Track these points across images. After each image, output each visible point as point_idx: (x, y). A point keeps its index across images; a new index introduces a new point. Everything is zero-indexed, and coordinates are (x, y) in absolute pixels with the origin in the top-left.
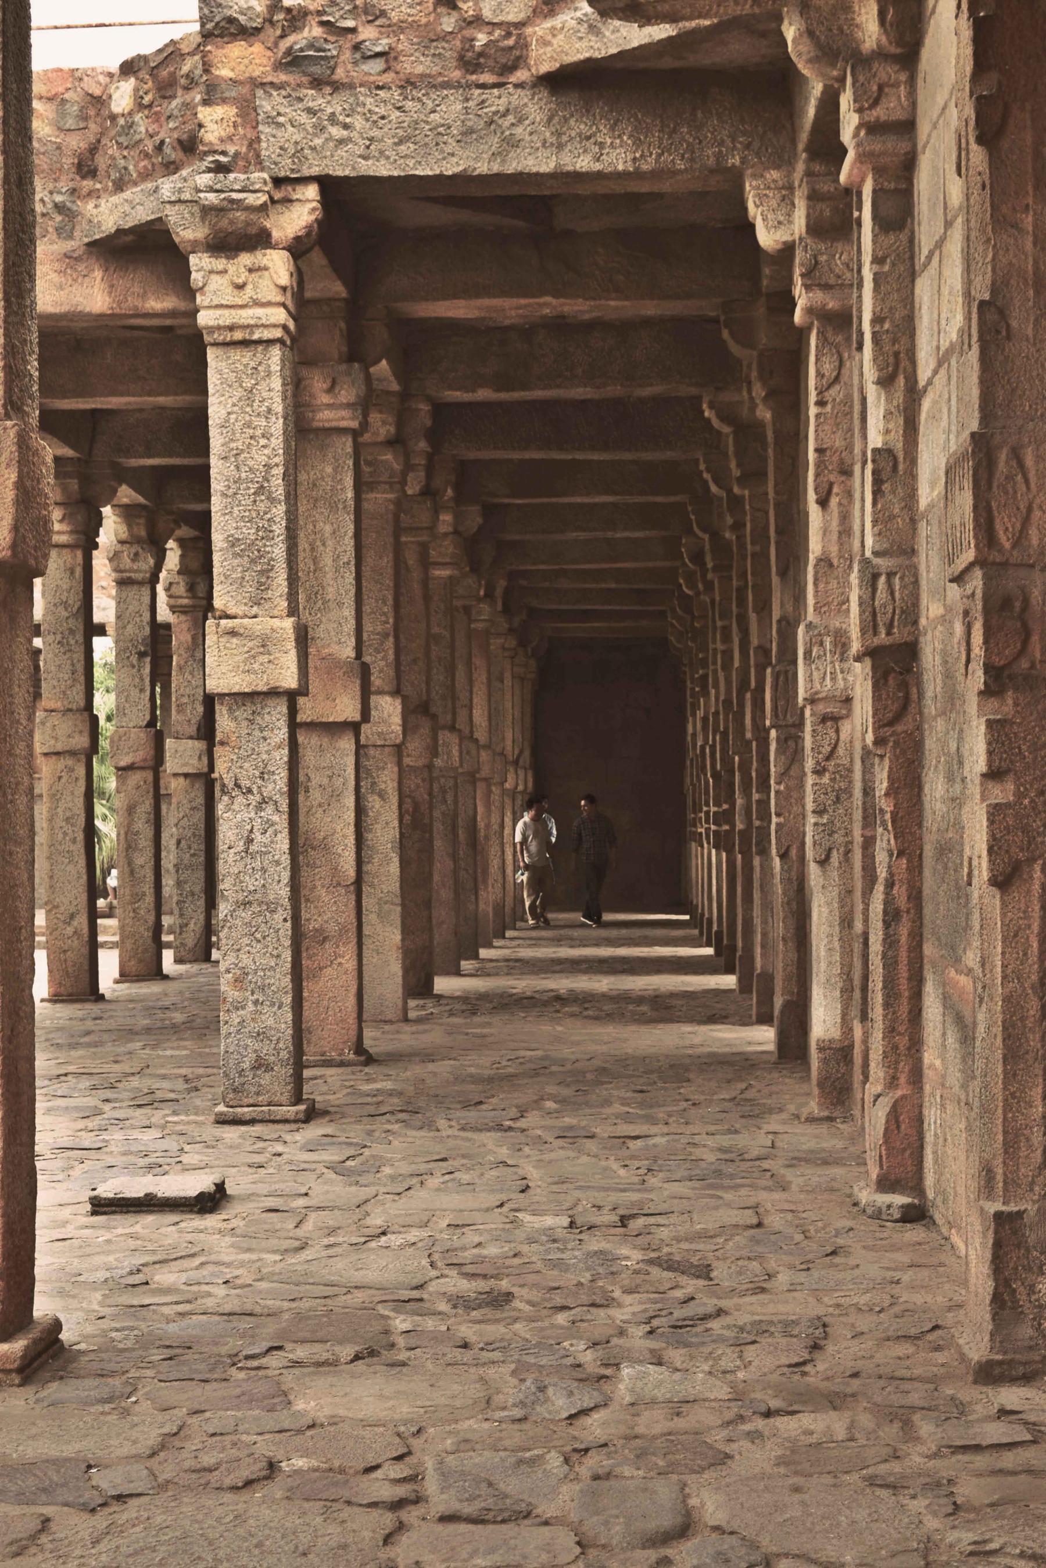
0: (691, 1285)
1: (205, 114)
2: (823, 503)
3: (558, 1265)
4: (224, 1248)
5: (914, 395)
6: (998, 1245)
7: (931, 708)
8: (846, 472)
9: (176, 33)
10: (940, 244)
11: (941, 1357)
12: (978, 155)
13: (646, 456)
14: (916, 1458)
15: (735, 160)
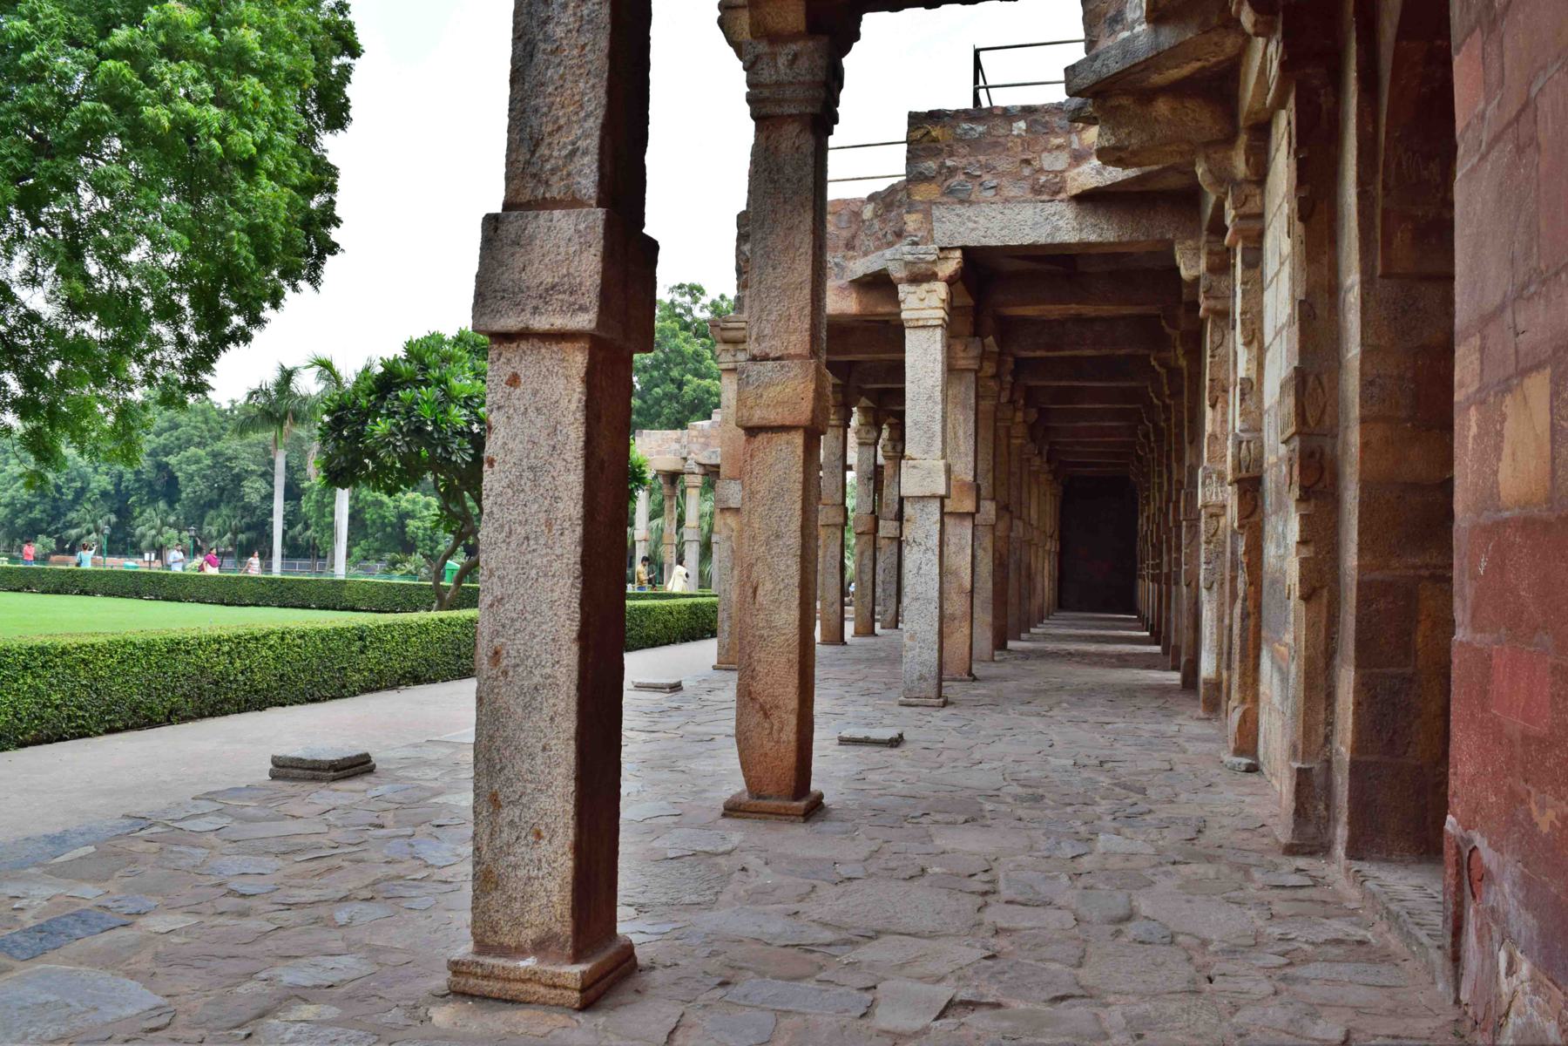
0: (1135, 797)
1: (908, 218)
2: (1213, 406)
3: (1069, 783)
4: (902, 765)
5: (1262, 351)
6: (1298, 785)
7: (1268, 508)
8: (1226, 391)
9: (895, 181)
10: (1277, 274)
11: (1266, 840)
12: (1299, 227)
13: (1121, 384)
14: (1251, 890)
15: (1169, 236)
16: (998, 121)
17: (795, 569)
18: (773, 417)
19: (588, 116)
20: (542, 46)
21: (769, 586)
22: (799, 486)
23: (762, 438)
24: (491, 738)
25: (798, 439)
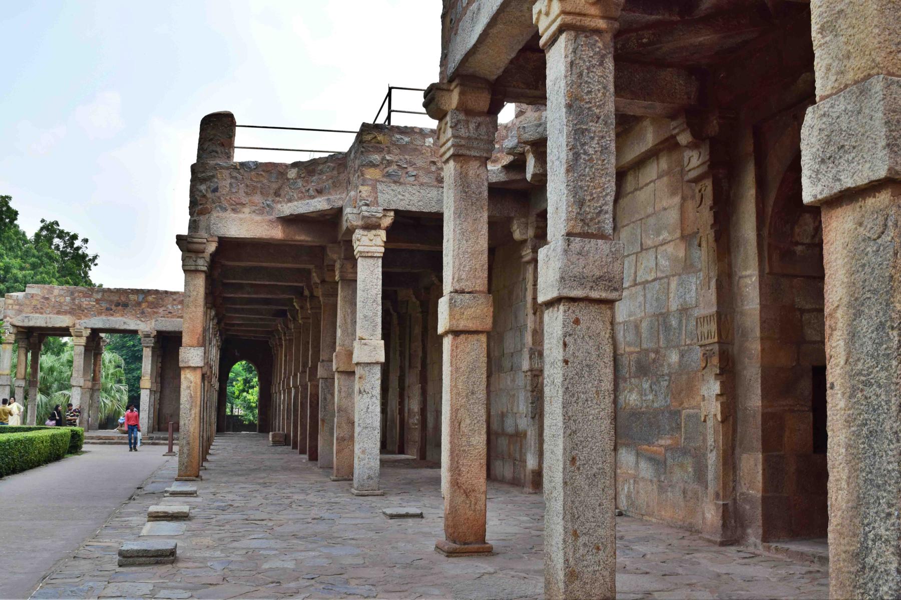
15: (512, 215)
16: (417, 136)
17: (483, 412)
18: (471, 325)
19: (607, 194)
20: (583, 156)
21: (468, 421)
22: (485, 365)
23: (462, 337)
24: (573, 502)
25: (483, 338)
